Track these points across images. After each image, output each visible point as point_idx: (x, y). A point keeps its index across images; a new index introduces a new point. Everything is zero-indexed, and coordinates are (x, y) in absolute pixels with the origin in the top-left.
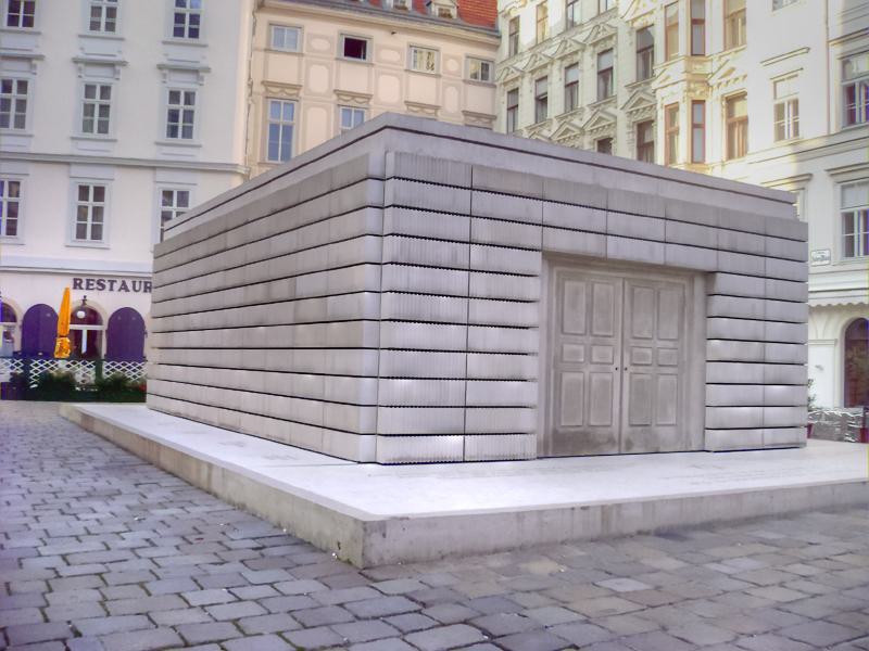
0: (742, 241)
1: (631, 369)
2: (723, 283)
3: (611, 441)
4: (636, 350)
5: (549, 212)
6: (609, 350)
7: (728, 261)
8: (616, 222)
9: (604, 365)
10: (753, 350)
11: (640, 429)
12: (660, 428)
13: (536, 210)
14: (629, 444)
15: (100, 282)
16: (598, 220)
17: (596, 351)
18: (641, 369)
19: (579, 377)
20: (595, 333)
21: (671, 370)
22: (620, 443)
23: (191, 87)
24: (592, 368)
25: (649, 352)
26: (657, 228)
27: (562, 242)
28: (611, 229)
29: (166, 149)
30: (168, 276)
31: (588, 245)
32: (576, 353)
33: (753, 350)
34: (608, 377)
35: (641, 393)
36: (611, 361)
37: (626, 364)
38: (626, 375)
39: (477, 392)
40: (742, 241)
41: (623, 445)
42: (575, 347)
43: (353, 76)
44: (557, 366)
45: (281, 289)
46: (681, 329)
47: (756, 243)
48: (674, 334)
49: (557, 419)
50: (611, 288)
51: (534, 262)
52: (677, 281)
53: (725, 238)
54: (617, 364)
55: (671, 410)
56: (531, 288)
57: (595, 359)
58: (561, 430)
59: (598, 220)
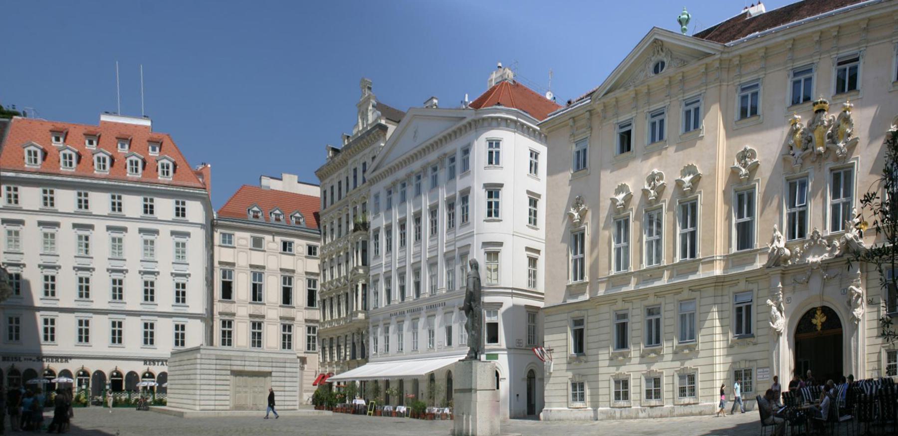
0: (278, 364)
5: (232, 362)
7: (274, 369)
8: (247, 363)
9: (246, 392)
10: (282, 389)
13: (229, 362)
15: (153, 361)
16: (243, 363)
23: (183, 282)
26: (257, 364)
30: (174, 359)
31: (241, 368)
39: (217, 398)
40: (278, 364)
43: (257, 258)
45: (189, 377)
47: (282, 365)
51: (229, 372)
53: (274, 364)
56: (228, 377)
59: (243, 363)
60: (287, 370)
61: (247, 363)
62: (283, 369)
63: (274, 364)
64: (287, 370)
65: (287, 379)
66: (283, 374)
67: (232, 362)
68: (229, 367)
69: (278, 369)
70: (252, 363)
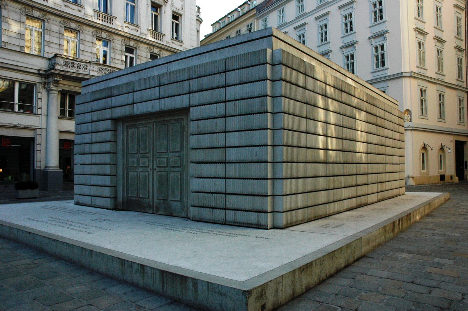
0: (205, 82)
1: (157, 169)
2: (194, 113)
3: (150, 206)
4: (158, 159)
6: (146, 160)
7: (196, 98)
10: (217, 155)
11: (162, 201)
12: (172, 202)
14: (158, 209)
17: (141, 161)
18: (162, 169)
19: (135, 174)
20: (141, 152)
21: (177, 169)
22: (153, 208)
24: (141, 169)
25: (165, 160)
27: (118, 113)
28: (136, 101)
29: (375, 74)
31: (126, 111)
32: (133, 162)
33: (217, 155)
34: (147, 174)
35: (161, 182)
36: (147, 165)
37: (155, 167)
38: (155, 172)
40: (205, 82)
41: (155, 209)
42: (133, 159)
44: (127, 169)
46: (182, 146)
47: (219, 80)
48: (178, 148)
49: (127, 193)
50: (147, 129)
51: (108, 124)
52: (180, 117)
53: (195, 84)
54: (151, 167)
55: (177, 193)
57: (141, 165)
58: (130, 198)
59: (131, 98)
60: (232, 92)
61: (137, 96)
62: (220, 94)
63: (195, 84)
64: (232, 92)
65: (233, 123)
66: (221, 108)
67: (112, 101)
68: (107, 114)
69: (207, 96)
70: (147, 94)
